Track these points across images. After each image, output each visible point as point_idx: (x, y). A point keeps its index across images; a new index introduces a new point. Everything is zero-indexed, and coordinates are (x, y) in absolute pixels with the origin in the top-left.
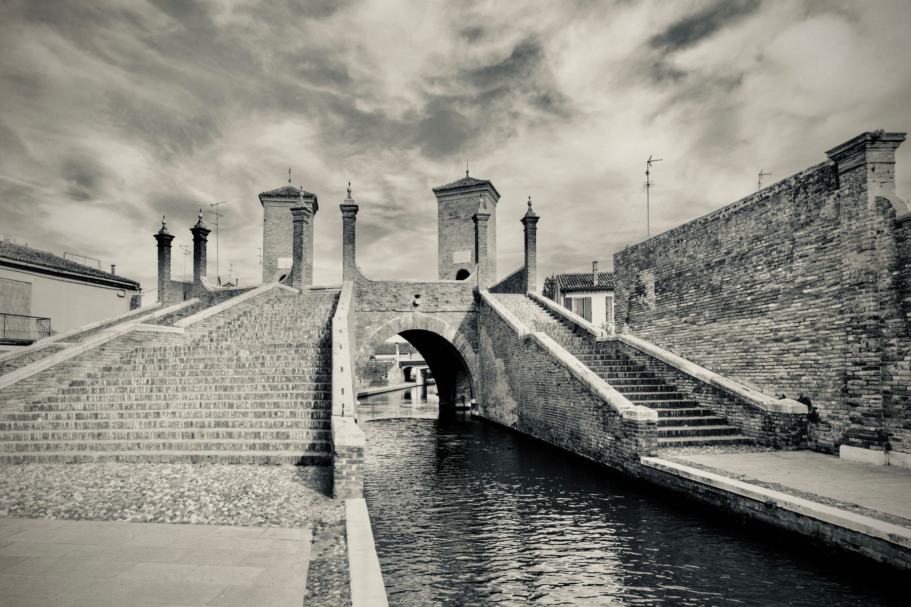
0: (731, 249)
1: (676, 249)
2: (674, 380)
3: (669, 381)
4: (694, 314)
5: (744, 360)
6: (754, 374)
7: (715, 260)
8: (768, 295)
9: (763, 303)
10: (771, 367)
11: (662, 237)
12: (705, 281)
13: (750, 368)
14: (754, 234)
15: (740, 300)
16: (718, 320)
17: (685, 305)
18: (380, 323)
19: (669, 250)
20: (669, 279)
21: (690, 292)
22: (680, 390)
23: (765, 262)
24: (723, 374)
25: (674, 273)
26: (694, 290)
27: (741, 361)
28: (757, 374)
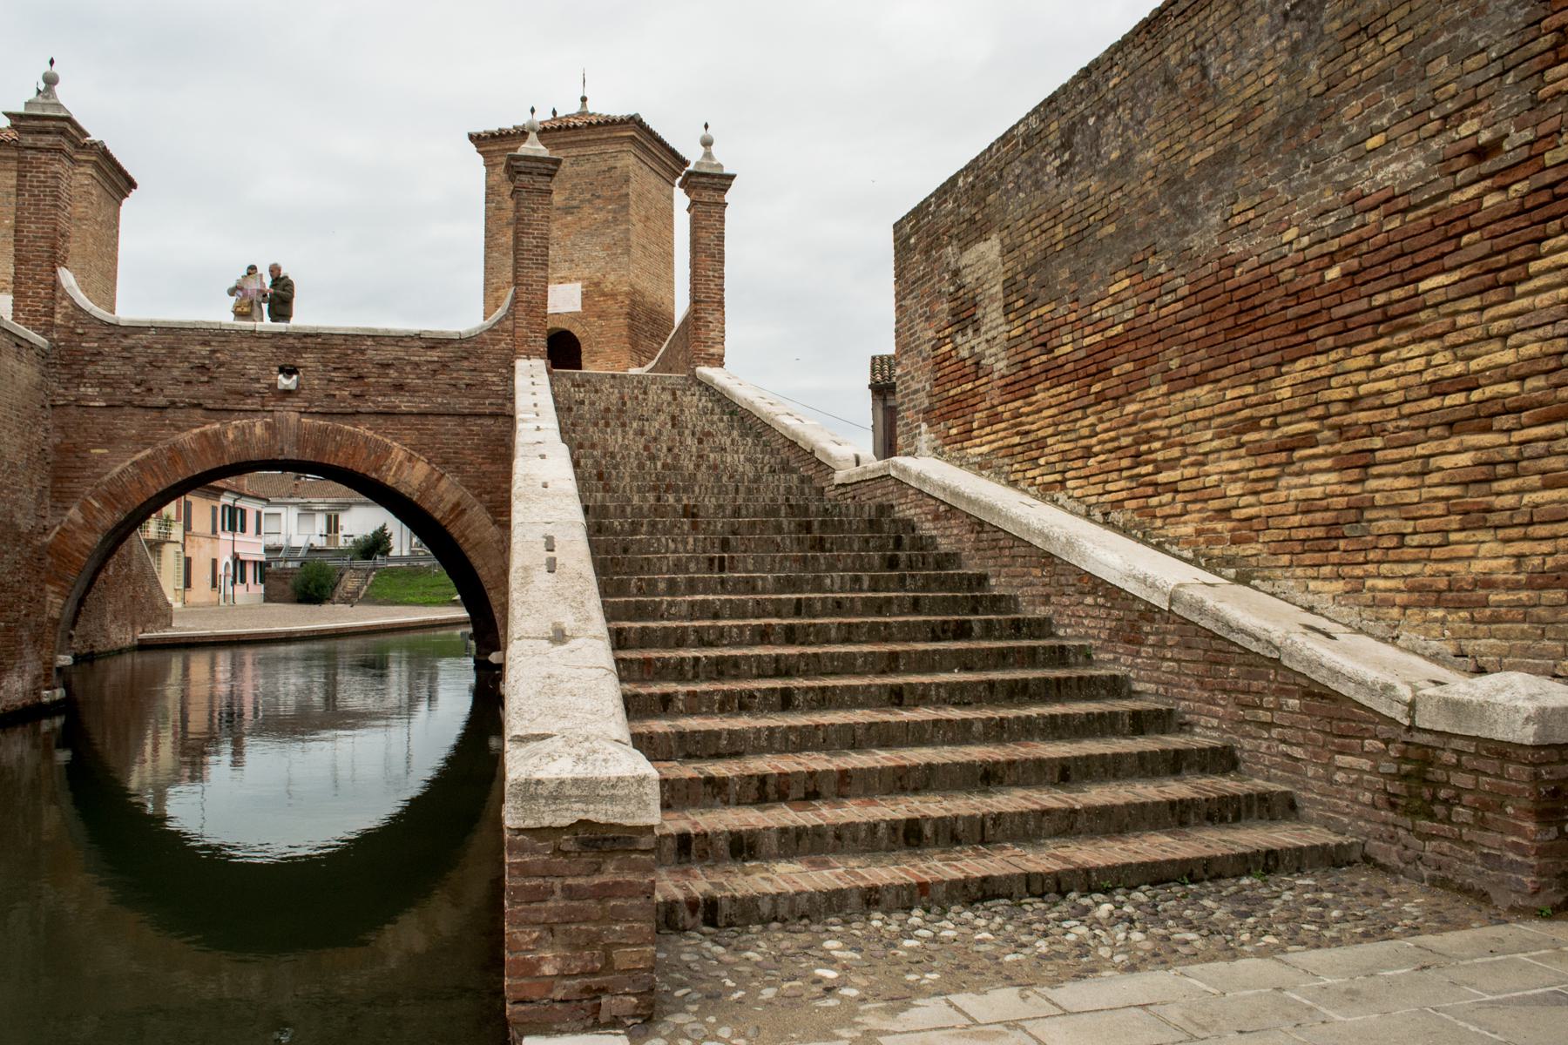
0: (1255, 101)
1: (1066, 156)
2: (1048, 596)
3: (1033, 603)
4: (1129, 366)
5: (1318, 517)
6: (1358, 571)
7: (1198, 158)
8: (1415, 243)
9: (1396, 280)
10: (1436, 539)
11: (1022, 128)
12: (1165, 242)
13: (1342, 544)
14: (1349, 15)
15: (1299, 284)
16: (1212, 375)
17: (1098, 337)
18: (143, 441)
19: (1044, 165)
20: (1046, 258)
21: (1112, 290)
22: (1068, 635)
23: (1399, 118)
24: (1232, 572)
25: (1060, 236)
26: (1126, 282)
27: (1306, 519)
28: (1371, 568)
